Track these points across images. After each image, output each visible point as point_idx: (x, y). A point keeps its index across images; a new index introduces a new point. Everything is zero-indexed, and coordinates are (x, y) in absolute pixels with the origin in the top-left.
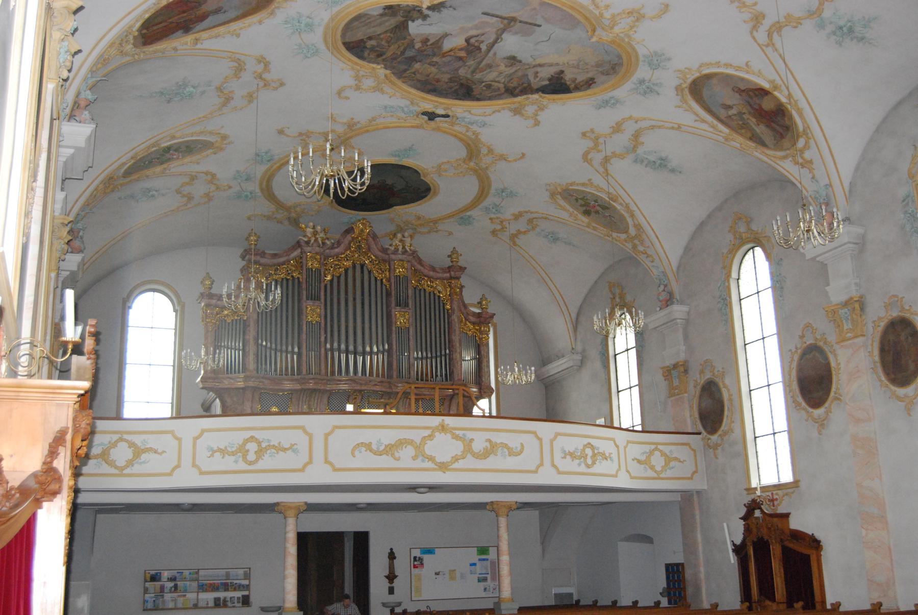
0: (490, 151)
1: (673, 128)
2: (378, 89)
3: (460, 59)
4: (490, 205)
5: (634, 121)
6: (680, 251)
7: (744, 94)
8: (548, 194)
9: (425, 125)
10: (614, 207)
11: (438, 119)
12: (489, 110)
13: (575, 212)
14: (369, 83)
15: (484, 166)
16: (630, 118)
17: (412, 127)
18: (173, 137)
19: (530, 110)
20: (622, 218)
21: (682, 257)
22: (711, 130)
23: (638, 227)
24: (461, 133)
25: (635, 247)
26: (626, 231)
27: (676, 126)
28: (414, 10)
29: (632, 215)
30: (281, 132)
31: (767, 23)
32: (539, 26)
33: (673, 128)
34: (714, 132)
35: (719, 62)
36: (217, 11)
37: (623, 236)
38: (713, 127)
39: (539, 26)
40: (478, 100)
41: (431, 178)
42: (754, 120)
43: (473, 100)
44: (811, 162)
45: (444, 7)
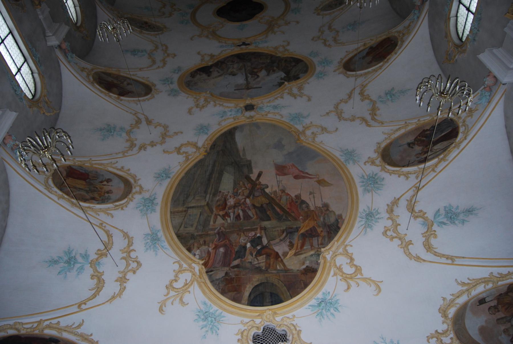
0: (207, 37)
1: (143, 68)
2: (276, 48)
3: (254, 68)
10: (138, 28)
11: (241, 43)
14: (281, 49)
16: (162, 67)
17: (250, 38)
18: (342, 9)
19: (207, 58)
27: (142, 70)
30: (298, 22)
32: (235, 90)
36: (364, 58)
39: (235, 90)
40: (232, 56)
44: (82, 71)
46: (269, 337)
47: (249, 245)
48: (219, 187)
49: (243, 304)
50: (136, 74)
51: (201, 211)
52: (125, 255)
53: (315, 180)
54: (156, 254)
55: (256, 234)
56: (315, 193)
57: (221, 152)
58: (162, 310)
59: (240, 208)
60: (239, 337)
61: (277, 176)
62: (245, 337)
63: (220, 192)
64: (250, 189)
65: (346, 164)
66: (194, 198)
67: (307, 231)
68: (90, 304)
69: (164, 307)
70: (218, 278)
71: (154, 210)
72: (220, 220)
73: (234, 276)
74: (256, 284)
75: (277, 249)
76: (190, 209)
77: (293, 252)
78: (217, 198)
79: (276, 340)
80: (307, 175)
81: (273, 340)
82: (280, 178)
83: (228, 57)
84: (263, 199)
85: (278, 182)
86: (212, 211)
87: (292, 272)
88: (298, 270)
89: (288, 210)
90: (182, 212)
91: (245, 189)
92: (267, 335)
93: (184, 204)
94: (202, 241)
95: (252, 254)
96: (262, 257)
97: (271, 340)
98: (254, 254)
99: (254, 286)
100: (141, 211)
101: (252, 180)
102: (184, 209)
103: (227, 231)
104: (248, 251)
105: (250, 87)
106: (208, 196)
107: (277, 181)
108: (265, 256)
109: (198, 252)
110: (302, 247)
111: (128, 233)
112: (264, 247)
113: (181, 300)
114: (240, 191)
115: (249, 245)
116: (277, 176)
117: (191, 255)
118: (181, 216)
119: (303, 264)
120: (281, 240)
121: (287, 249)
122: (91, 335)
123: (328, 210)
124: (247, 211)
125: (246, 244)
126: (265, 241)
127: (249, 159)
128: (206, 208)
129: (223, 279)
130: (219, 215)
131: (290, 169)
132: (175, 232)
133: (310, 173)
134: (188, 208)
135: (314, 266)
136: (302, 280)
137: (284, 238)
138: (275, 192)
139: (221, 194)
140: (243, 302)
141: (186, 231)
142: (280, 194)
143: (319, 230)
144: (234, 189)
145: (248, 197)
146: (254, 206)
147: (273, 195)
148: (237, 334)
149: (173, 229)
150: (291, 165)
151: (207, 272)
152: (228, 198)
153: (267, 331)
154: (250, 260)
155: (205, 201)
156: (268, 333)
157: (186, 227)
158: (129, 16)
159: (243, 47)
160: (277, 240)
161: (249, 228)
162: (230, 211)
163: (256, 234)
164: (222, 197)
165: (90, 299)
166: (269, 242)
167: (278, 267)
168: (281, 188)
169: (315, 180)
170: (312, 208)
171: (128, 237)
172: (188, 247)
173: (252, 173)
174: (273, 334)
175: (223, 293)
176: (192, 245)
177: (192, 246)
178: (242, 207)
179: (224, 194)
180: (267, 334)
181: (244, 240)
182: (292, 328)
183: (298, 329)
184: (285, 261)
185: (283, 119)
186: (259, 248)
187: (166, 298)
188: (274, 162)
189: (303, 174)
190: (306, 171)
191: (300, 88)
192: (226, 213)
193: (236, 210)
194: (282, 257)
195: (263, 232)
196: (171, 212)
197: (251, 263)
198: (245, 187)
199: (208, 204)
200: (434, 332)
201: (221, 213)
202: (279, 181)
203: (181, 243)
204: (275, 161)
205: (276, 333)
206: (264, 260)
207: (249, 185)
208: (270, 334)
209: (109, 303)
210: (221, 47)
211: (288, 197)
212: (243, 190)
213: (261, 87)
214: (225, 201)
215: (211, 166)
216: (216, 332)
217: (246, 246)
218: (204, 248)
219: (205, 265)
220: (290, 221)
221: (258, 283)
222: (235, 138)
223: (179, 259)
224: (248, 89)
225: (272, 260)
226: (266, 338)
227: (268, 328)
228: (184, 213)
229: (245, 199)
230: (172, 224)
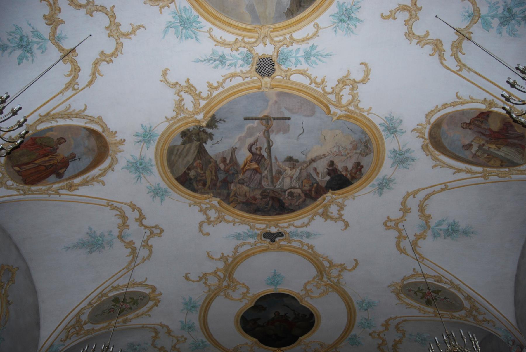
1: (442, 190)
2: (220, 219)
3: (256, 171)
4: (362, 320)
5: (412, 196)
6: (512, 308)
7: (472, 126)
8: (393, 295)
9: (270, 246)
12: (306, 220)
13: (422, 306)
15: (335, 280)
16: (408, 194)
18: (114, 288)
19: (333, 210)
20: (456, 297)
21: (516, 313)
22: (469, 176)
23: (469, 298)
24: (299, 248)
25: (475, 318)
26: (461, 307)
27: (443, 186)
28: (200, 131)
29: (459, 290)
31: (447, 47)
32: (289, 119)
33: (442, 190)
34: (472, 176)
35: (437, 106)
36: (73, 157)
37: (463, 313)
38: (468, 172)
39: (289, 119)
40: (293, 211)
41: (309, 302)
42: (494, 146)
43: (288, 213)
45: (217, 121)
50: (454, 173)
83: (300, 207)
105: (264, 122)
158: (456, 314)
159: (274, 230)
185: (208, 25)
191: (179, 107)
210: (308, 235)
213: (246, 119)
224: (267, 119)
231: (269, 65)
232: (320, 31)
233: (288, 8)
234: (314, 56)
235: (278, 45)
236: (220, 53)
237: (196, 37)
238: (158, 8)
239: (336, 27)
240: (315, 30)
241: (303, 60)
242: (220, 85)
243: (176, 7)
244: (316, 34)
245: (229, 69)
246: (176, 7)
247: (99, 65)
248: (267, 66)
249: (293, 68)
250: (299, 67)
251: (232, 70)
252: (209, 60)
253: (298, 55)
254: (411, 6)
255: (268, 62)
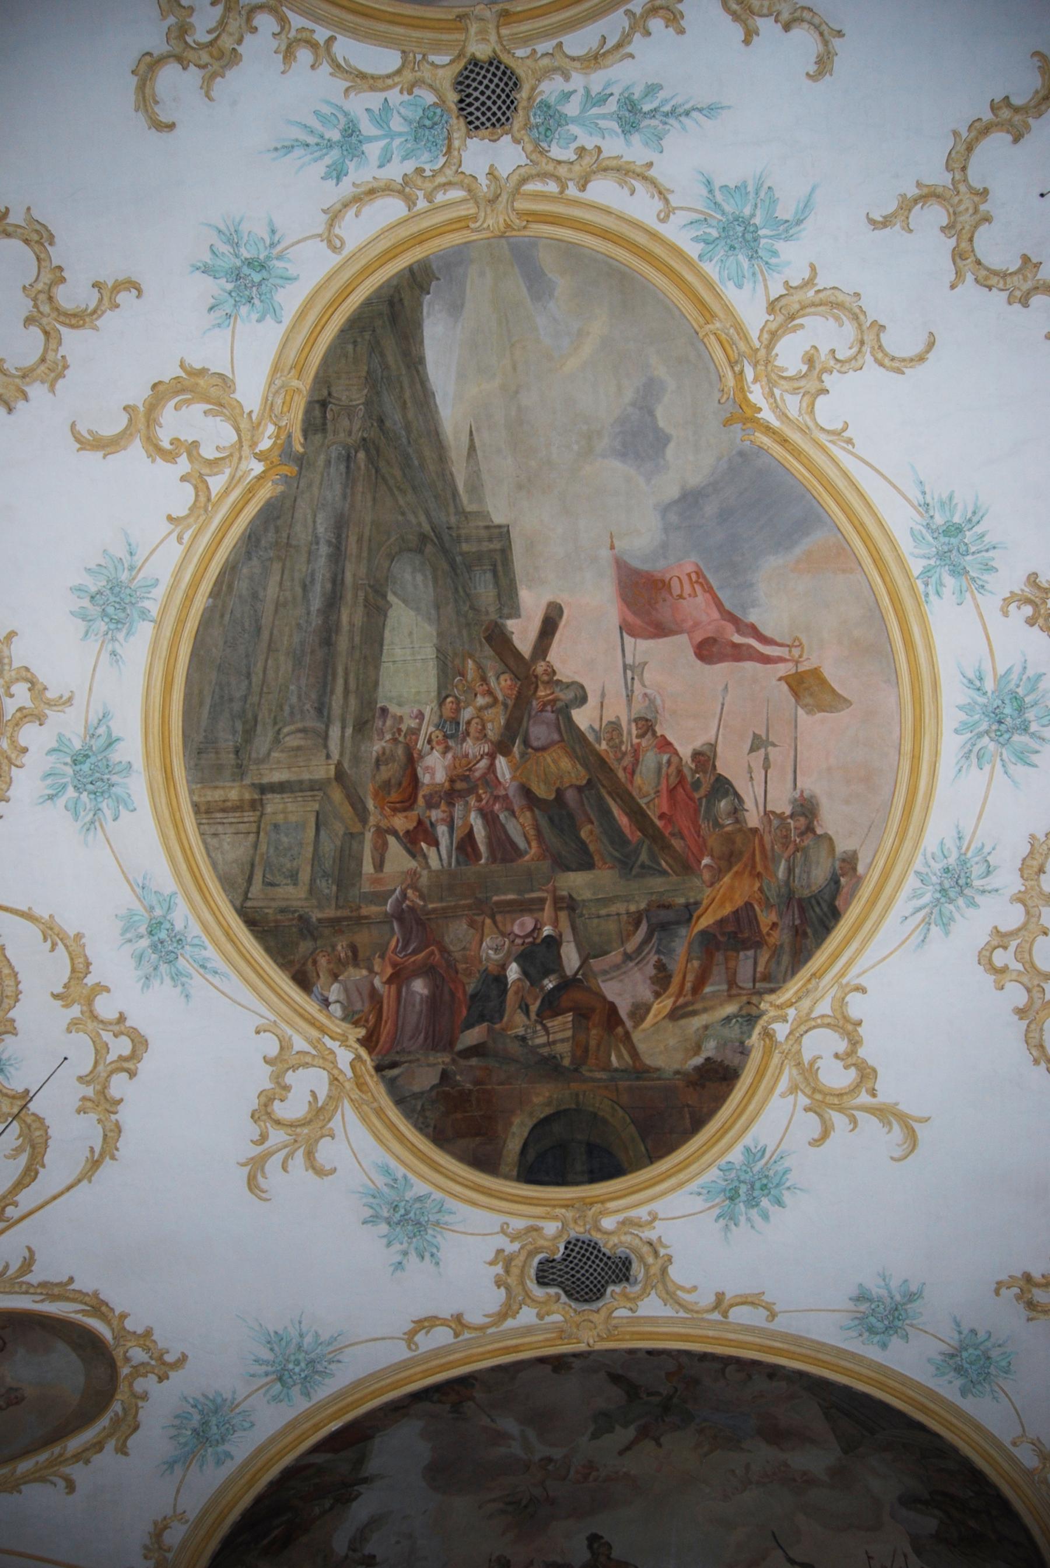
46: (582, 1268)
47: (513, 972)
48: (376, 684)
49: (507, 1177)
51: (316, 806)
52: (76, 1011)
53: (783, 669)
54: (187, 996)
55: (537, 928)
56: (774, 745)
57: (361, 455)
58: (258, 1187)
59: (472, 801)
60: (499, 1269)
61: (625, 635)
62: (515, 1271)
63: (384, 711)
64: (510, 703)
65: (927, 595)
66: (277, 741)
67: (721, 922)
68: (27, 1199)
69: (259, 1176)
70: (416, 1089)
71: (124, 802)
72: (396, 853)
73: (468, 1086)
74: (542, 1116)
75: (611, 990)
76: (269, 796)
77: (666, 1003)
78: (377, 747)
79: (599, 1274)
80: (753, 642)
81: (592, 1274)
82: (641, 648)
84: (566, 764)
85: (629, 674)
86: (362, 815)
87: (659, 1079)
88: (677, 1072)
89: (659, 823)
90: (238, 808)
91: (488, 706)
92: (576, 1261)
93: (240, 771)
94: (341, 948)
95: (527, 1006)
96: (560, 1018)
97: (587, 1275)
98: (534, 1008)
99: (535, 1121)
100: (74, 809)
101: (517, 655)
102: (247, 796)
103: (430, 906)
104: (510, 996)
106: (335, 732)
107: (625, 667)
108: (569, 1017)
109: (335, 992)
110: (697, 989)
111: (57, 918)
112: (567, 984)
113: (310, 1155)
114: (467, 714)
115: (513, 972)
116: (627, 638)
117: (312, 1007)
118: (242, 827)
119: (698, 1049)
120: (628, 957)
121: (645, 993)
122: (71, 1280)
123: (810, 829)
124: (502, 817)
125: (504, 967)
126: (571, 958)
127: (498, 519)
128: (337, 794)
129: (434, 1093)
130: (395, 833)
131: (681, 597)
132: (231, 902)
133: (767, 632)
134: (264, 789)
135: (731, 1059)
136: (688, 1106)
137: (639, 949)
138: (615, 726)
139: (389, 723)
140: (504, 1169)
141: (273, 899)
142: (635, 741)
143: (766, 918)
144: (441, 703)
145: (502, 747)
146: (526, 792)
147: (604, 746)
148: (492, 1263)
149: (225, 891)
150: (689, 575)
151: (379, 1069)
152: (419, 746)
153: (577, 1249)
154: (521, 1031)
155: (328, 757)
156: (579, 1257)
157: (272, 885)
160: (615, 956)
161: (511, 897)
162: (435, 815)
163: (537, 928)
164: (395, 740)
165: (20, 1185)
166: (584, 962)
167: (613, 1058)
168: (639, 707)
169: (783, 669)
170: (753, 819)
171: (62, 936)
172: (297, 967)
173: (515, 613)
174: (592, 1258)
175: (440, 1138)
176: (310, 961)
177: (309, 966)
178: (479, 799)
179: (404, 727)
180: (575, 1258)
181: (496, 950)
182: (645, 1249)
183: (662, 1252)
184: (637, 1036)
186: (551, 986)
187: (259, 1149)
188: (612, 547)
189: (738, 631)
190: (753, 617)
192: (420, 822)
193: (458, 811)
194: (629, 1024)
195: (563, 915)
196: (196, 807)
197: (523, 1039)
198: (490, 692)
199: (340, 776)
200: (1019, 1275)
201: (401, 823)
202: (632, 668)
203: (268, 950)
204: (616, 543)
205: (601, 1256)
206: (569, 1033)
207: (506, 681)
208: (584, 1260)
209: (85, 1182)
211: (665, 758)
212: (481, 709)
214: (411, 761)
215: (324, 550)
216: (432, 1255)
217: (506, 977)
218: (356, 974)
219: (368, 1042)
220: (664, 873)
221: (548, 1111)
222: (421, 360)
223: (273, 1018)
225: (594, 1032)
226: (572, 1269)
227: (578, 1240)
228: (250, 816)
229: (492, 757)
230: (214, 865)
231: (477, 104)
232: (321, 229)
233: (428, 293)
234: (330, 145)
235: (449, 172)
236: (636, 138)
237: (711, 191)
238: (821, 282)
239: (272, 245)
240: (337, 230)
241: (367, 128)
242: (638, 25)
243: (766, 287)
244: (334, 216)
245: (608, 85)
246: (766, 287)
247: (1037, 92)
248: (483, 98)
249: (395, 96)
250: (374, 100)
251: (597, 80)
252: (673, 112)
253: (382, 143)
254: (58, 326)
255: (479, 114)
